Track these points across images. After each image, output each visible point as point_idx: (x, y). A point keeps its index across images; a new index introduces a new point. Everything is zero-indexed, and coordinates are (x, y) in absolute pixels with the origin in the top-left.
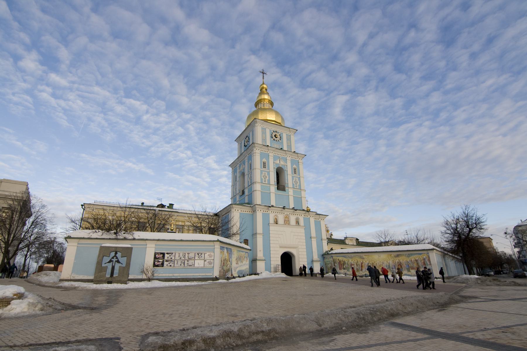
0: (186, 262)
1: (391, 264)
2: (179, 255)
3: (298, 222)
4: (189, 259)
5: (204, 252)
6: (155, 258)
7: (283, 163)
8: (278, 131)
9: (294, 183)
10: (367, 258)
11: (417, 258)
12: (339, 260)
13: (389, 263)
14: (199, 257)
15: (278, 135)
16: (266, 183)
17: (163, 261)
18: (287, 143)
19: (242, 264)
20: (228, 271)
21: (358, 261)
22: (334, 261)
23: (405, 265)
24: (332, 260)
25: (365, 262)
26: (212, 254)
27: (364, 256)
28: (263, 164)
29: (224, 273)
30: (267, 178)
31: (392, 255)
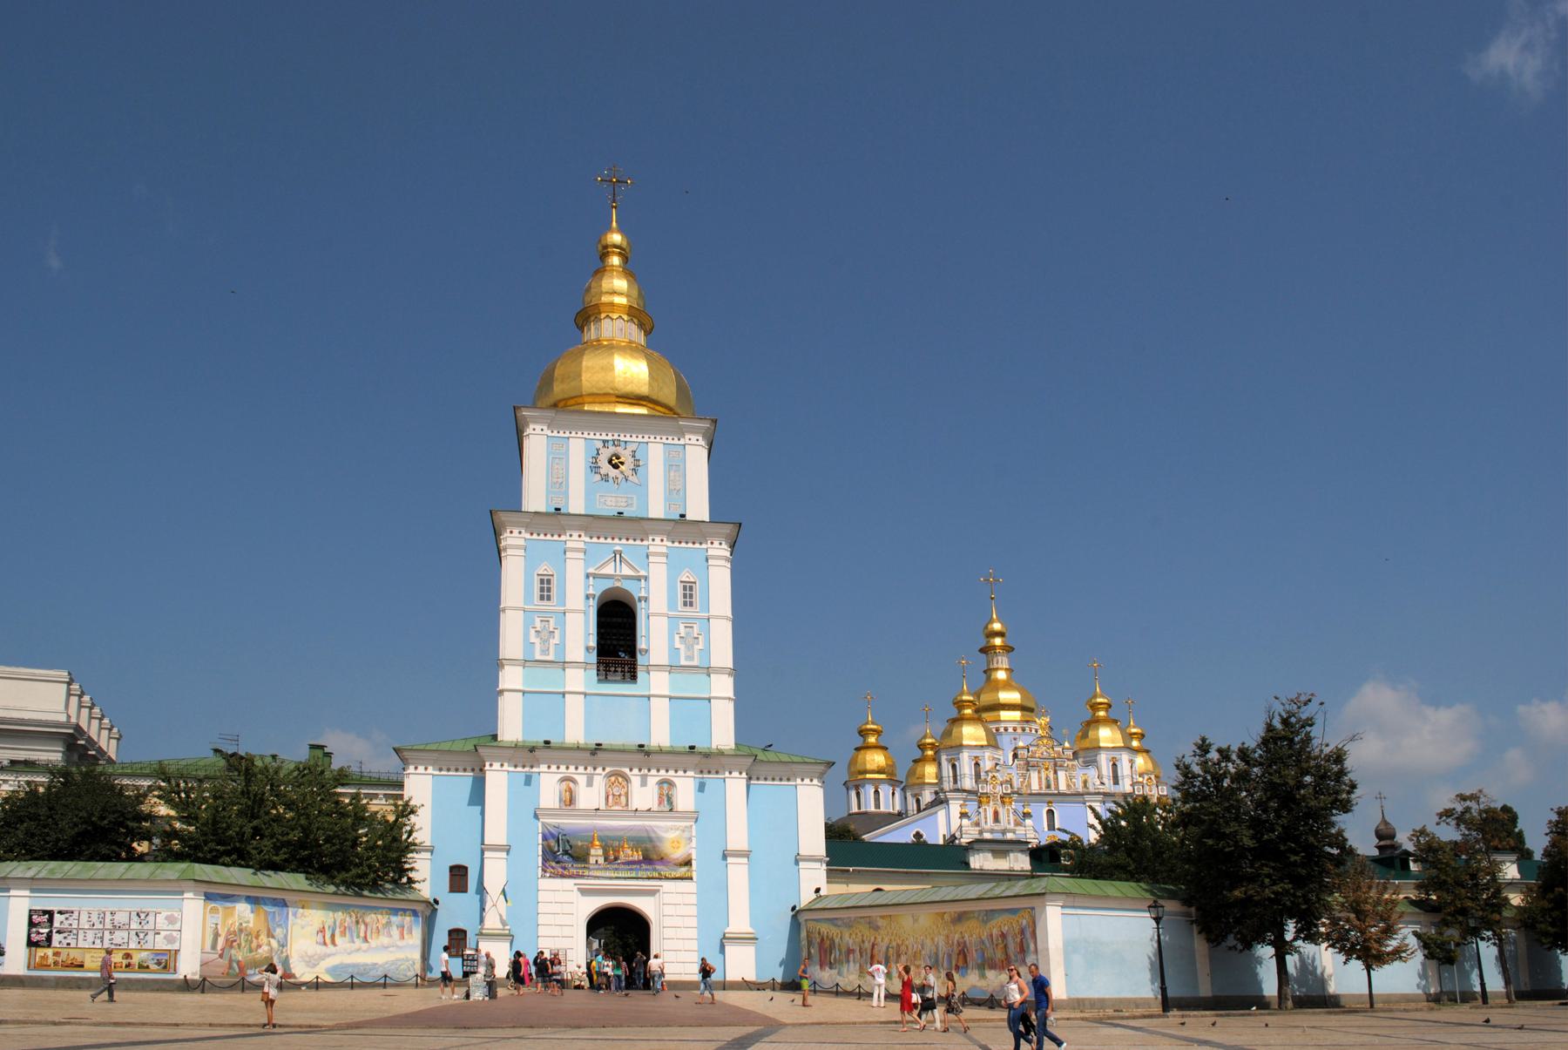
0: (107, 933)
1: (940, 949)
2: (90, 917)
5: (155, 910)
6: (31, 924)
10: (886, 928)
11: (1006, 928)
12: (819, 933)
13: (937, 949)
14: (140, 923)
17: (51, 932)
19: (365, 946)
21: (865, 938)
22: (808, 936)
23: (975, 955)
25: (880, 940)
26: (176, 914)
27: (878, 919)
29: (230, 967)
31: (945, 916)
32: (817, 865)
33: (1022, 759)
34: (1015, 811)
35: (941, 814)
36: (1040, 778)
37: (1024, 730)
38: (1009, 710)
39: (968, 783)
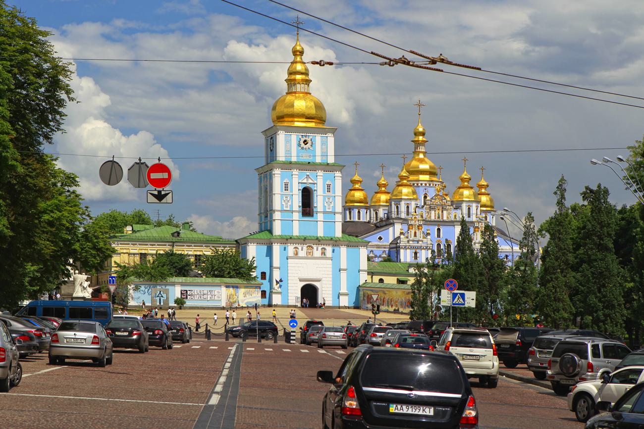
0: (202, 296)
3: (323, 253)
4: (204, 294)
7: (312, 182)
8: (309, 134)
9: (326, 205)
15: (308, 139)
16: (288, 209)
18: (322, 149)
20: (236, 302)
24: (362, 293)
26: (220, 291)
28: (284, 186)
30: (289, 204)
32: (365, 272)
33: (428, 205)
34: (423, 232)
35: (391, 229)
36: (435, 214)
37: (430, 185)
38: (423, 174)
39: (403, 216)
